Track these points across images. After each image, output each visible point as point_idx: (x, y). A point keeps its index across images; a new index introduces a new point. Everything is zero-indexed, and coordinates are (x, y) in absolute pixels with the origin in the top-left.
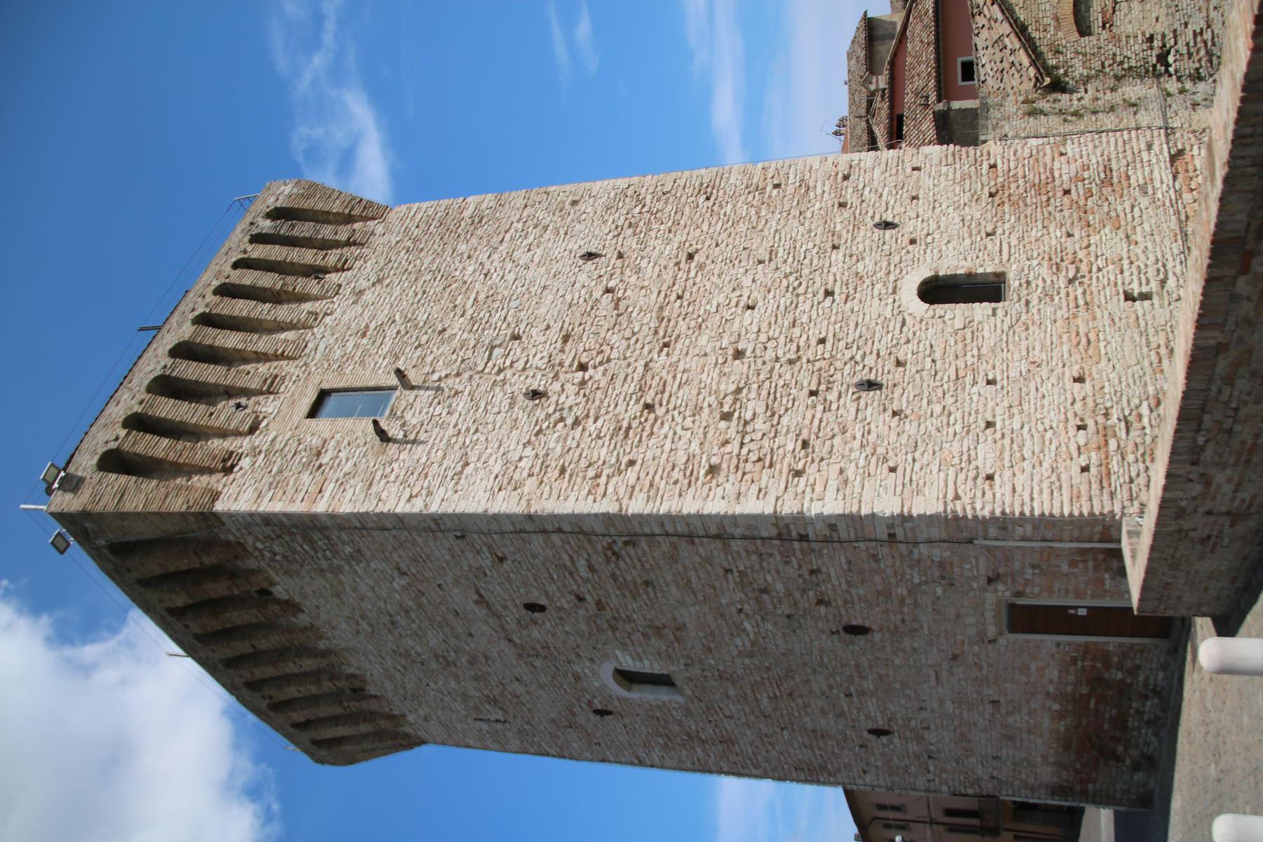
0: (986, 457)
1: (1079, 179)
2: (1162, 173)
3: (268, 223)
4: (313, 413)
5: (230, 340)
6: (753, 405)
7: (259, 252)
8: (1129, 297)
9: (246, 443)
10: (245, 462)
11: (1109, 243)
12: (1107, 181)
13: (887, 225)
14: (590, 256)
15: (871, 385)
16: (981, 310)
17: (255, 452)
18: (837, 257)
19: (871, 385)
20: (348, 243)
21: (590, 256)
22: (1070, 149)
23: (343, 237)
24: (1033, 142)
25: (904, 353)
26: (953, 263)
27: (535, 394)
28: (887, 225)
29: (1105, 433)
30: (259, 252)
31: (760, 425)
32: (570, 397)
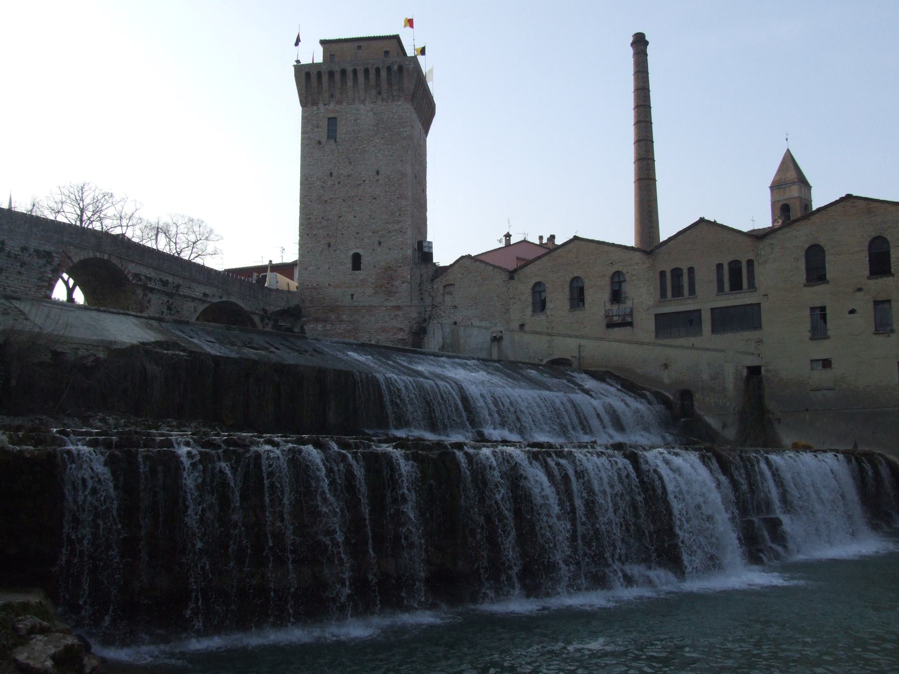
0: (311, 268)
1: (392, 286)
2: (392, 304)
3: (396, 67)
4: (329, 119)
5: (350, 83)
6: (325, 223)
7: (383, 73)
8: (352, 295)
9: (321, 106)
10: (315, 108)
11: (369, 291)
12: (391, 292)
13: (380, 243)
14: (378, 173)
15: (329, 245)
16: (350, 266)
17: (318, 109)
18: (370, 234)
19: (329, 245)
20: (393, 96)
21: (378, 173)
22: (404, 285)
23: (394, 93)
24: (409, 277)
25: (338, 251)
26: (364, 260)
27: (331, 174)
28: (380, 243)
29: (316, 289)
30: (383, 73)
31: (320, 226)
32: (329, 183)
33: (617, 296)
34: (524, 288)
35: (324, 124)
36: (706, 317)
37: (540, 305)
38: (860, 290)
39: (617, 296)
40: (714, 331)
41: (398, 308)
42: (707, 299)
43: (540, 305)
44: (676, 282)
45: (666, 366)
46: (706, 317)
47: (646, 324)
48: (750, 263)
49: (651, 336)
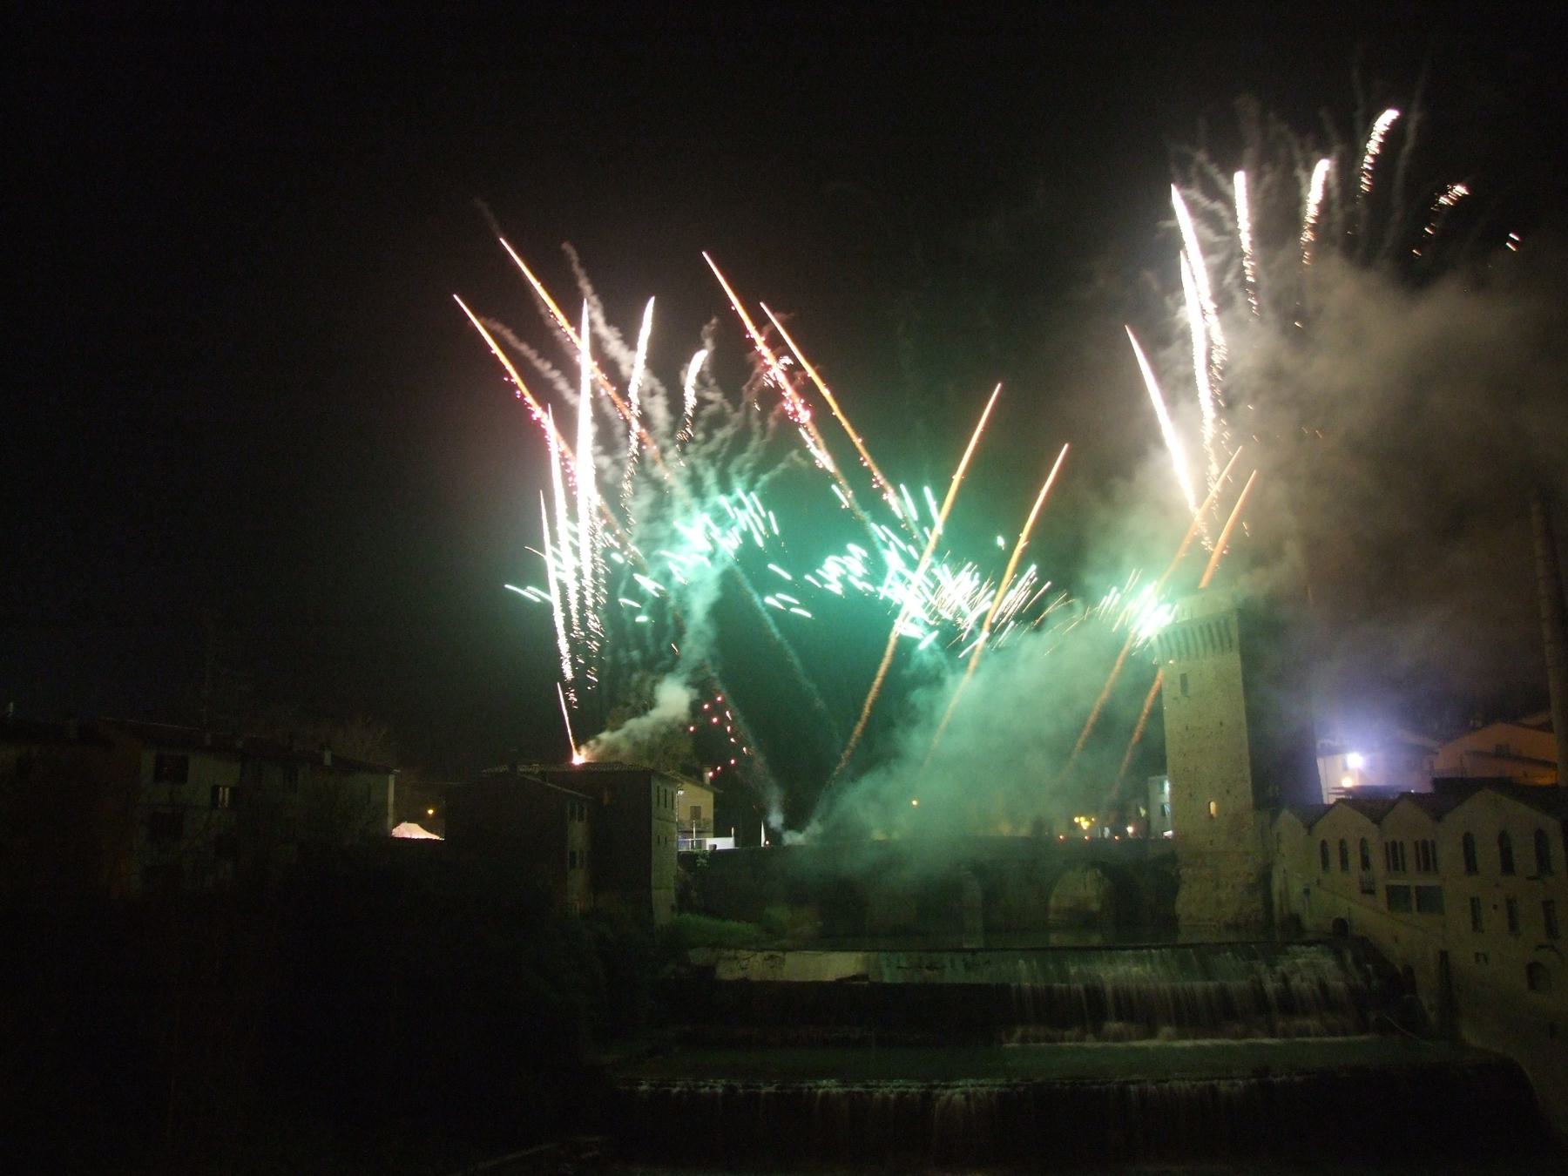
33: (1366, 864)
34: (1318, 843)
35: (1178, 681)
36: (1413, 892)
37: (1325, 863)
38: (1497, 885)
39: (1366, 864)
40: (1419, 909)
41: (1247, 853)
42: (1412, 879)
43: (1325, 863)
44: (1394, 854)
45: (1396, 940)
46: (1413, 892)
47: (1382, 894)
48: (1433, 845)
49: (1383, 905)
